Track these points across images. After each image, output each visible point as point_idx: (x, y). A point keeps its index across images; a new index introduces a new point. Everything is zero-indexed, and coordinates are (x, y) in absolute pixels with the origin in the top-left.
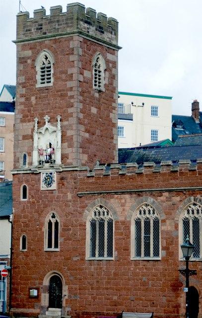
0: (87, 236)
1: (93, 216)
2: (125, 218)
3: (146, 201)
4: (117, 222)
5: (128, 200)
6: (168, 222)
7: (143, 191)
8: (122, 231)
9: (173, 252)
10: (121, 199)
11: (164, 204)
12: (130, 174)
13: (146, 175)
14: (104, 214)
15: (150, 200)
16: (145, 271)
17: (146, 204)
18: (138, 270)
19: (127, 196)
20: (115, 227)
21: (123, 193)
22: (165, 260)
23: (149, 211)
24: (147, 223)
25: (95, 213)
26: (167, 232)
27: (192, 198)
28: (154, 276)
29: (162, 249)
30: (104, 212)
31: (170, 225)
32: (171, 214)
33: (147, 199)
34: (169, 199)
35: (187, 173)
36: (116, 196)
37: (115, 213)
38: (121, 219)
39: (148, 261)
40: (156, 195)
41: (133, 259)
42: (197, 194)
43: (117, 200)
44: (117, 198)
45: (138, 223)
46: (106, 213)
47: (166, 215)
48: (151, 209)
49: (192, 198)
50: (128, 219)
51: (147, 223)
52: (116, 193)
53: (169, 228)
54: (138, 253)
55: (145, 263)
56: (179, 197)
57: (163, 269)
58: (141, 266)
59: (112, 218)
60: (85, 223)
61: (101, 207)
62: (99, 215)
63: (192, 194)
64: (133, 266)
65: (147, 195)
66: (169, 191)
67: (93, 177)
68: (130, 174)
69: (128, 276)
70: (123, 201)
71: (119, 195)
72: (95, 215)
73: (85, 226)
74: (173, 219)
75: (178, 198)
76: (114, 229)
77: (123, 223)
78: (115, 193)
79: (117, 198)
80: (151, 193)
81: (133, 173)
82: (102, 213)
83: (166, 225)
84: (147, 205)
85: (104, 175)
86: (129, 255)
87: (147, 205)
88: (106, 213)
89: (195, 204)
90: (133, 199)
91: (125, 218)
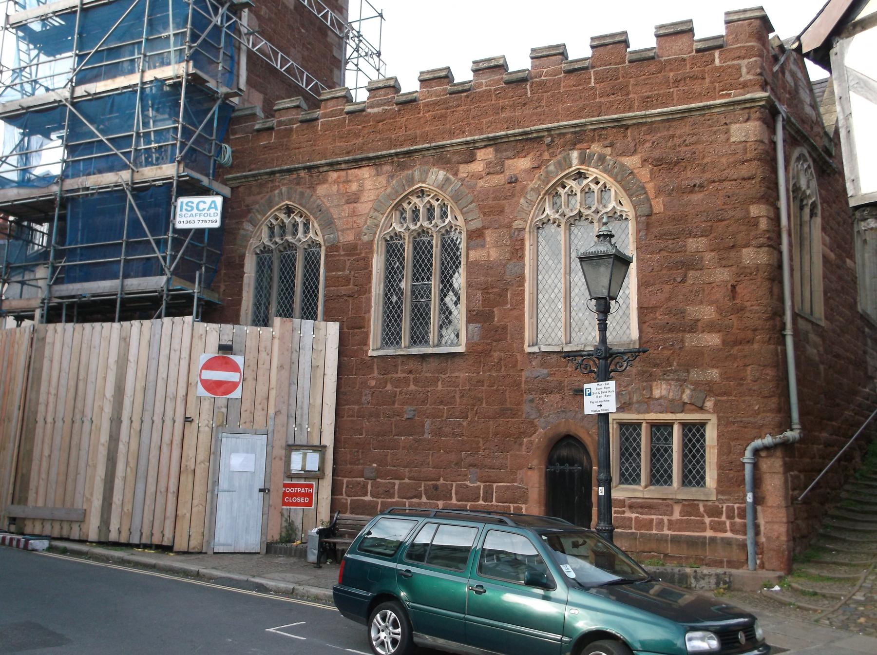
0: (245, 294)
1: (266, 240)
2: (358, 235)
3: (424, 182)
4: (332, 248)
5: (368, 185)
6: (490, 236)
7: (416, 151)
8: (347, 272)
9: (505, 328)
10: (347, 182)
11: (481, 183)
12: (376, 110)
13: (427, 105)
14: (295, 233)
15: (438, 175)
16: (412, 387)
17: (422, 191)
18: (389, 387)
19: (366, 173)
20: (326, 263)
21: (357, 163)
22: (477, 353)
23: (430, 210)
24: (422, 250)
25: (271, 228)
26: (486, 267)
27: (575, 155)
28: (441, 403)
29: (469, 321)
30: (295, 225)
31: (497, 245)
32: (502, 211)
33: (427, 173)
34: (493, 169)
35: (558, 83)
36: (334, 175)
37: (328, 224)
38: (349, 237)
39: (423, 357)
40: (455, 158)
41: (375, 354)
42: (593, 140)
43: (335, 188)
44: (336, 182)
45: (393, 250)
46: (301, 228)
47: (485, 214)
48: (435, 204)
49: (575, 155)
50: (366, 238)
51: (422, 250)
52: (333, 166)
53: (494, 254)
54: (391, 336)
55: (412, 365)
56: (528, 159)
57: (470, 379)
58: (400, 375)
59: (320, 239)
60: (242, 257)
61: (289, 211)
62: (283, 235)
63: (573, 145)
64: (376, 374)
65: (427, 163)
66: (493, 142)
67: (271, 129)
68: (376, 110)
69: (358, 402)
70: (354, 187)
71: (343, 173)
72: (272, 235)
73: (242, 266)
74: (509, 226)
75: (523, 163)
76: (322, 270)
77: (352, 249)
78: (331, 165)
79: (336, 182)
80: (441, 157)
81: (384, 104)
82: (289, 228)
83: (483, 246)
84: (421, 193)
85: (302, 122)
86: (365, 342)
87: (421, 193)
88: (301, 228)
89: (580, 175)
90: (382, 180)
91: (358, 235)
